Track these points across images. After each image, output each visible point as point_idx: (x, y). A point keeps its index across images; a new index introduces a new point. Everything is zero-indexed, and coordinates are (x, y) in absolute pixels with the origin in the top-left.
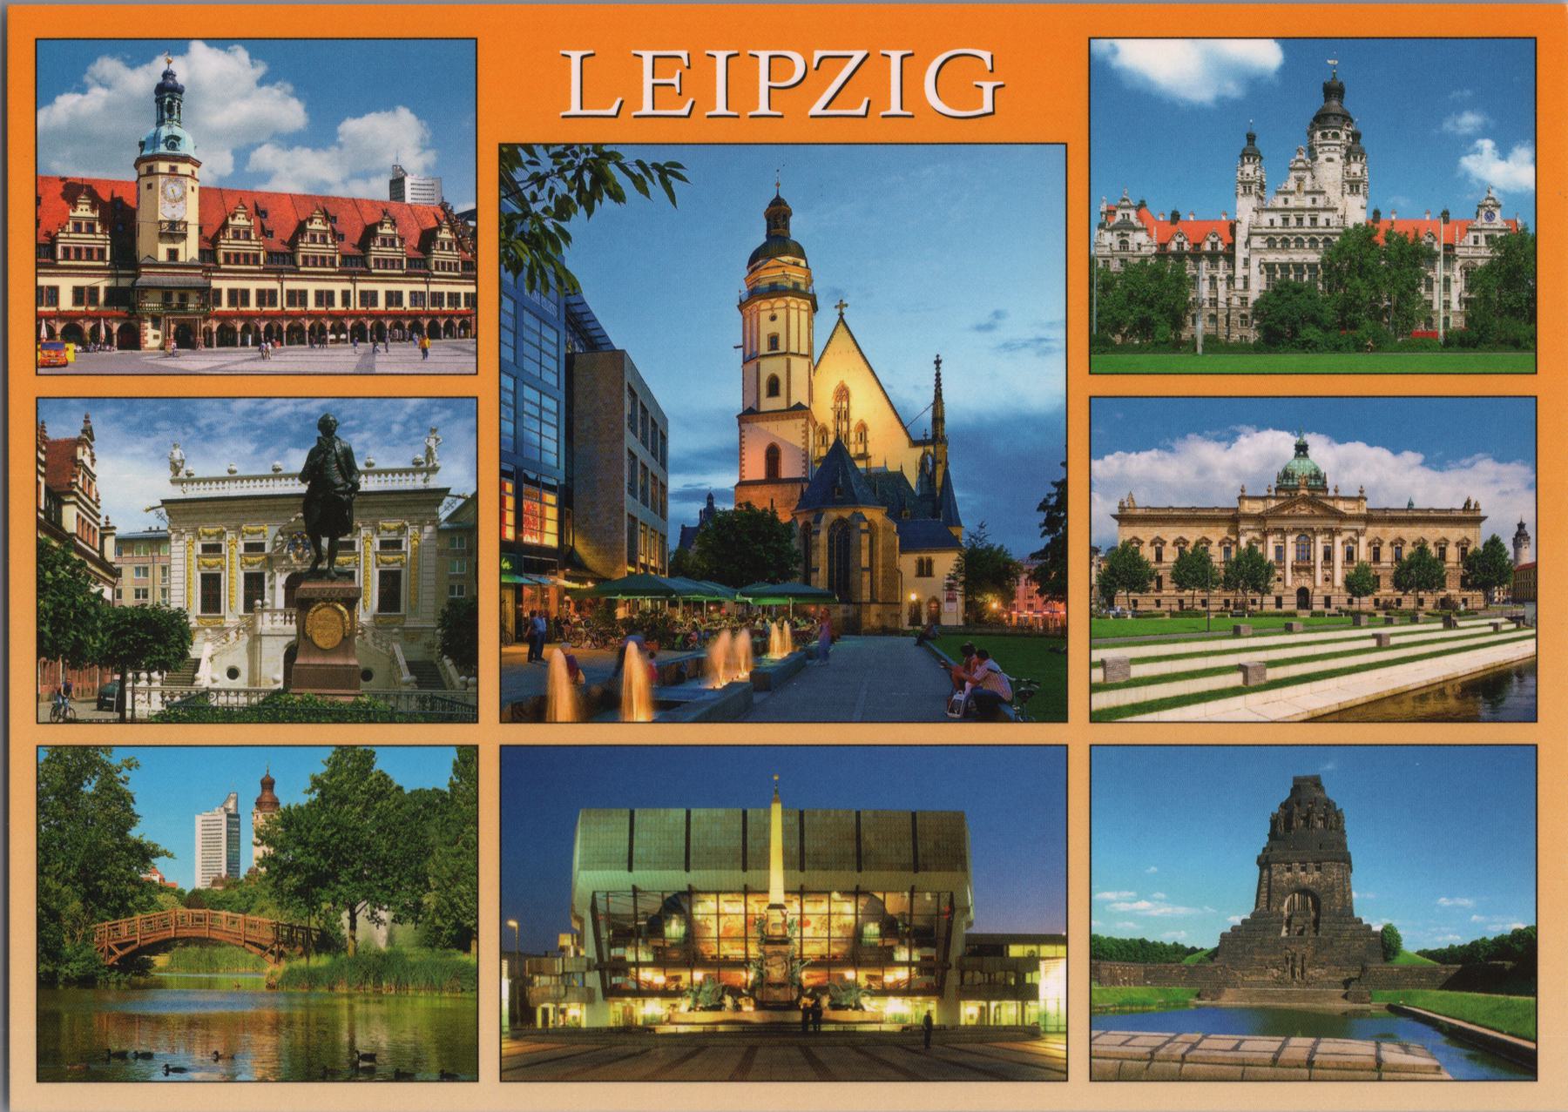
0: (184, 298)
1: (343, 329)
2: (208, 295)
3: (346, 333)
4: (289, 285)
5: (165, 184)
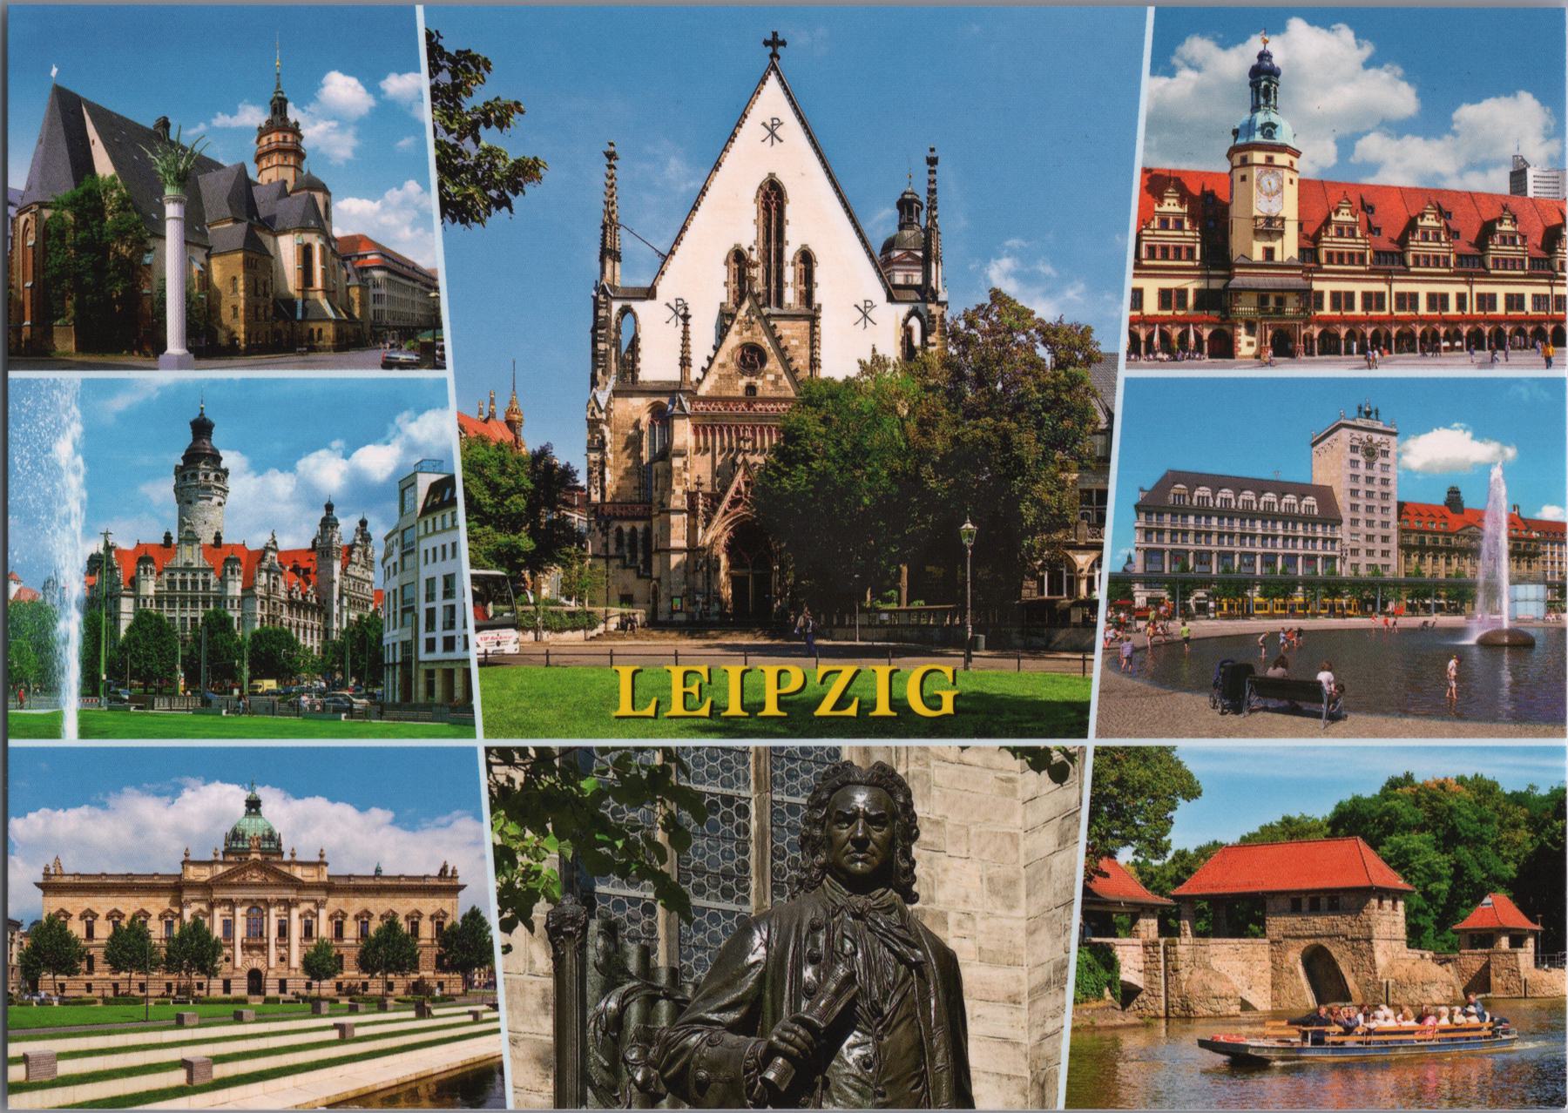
0: (1281, 302)
3: (1460, 339)
4: (1398, 287)
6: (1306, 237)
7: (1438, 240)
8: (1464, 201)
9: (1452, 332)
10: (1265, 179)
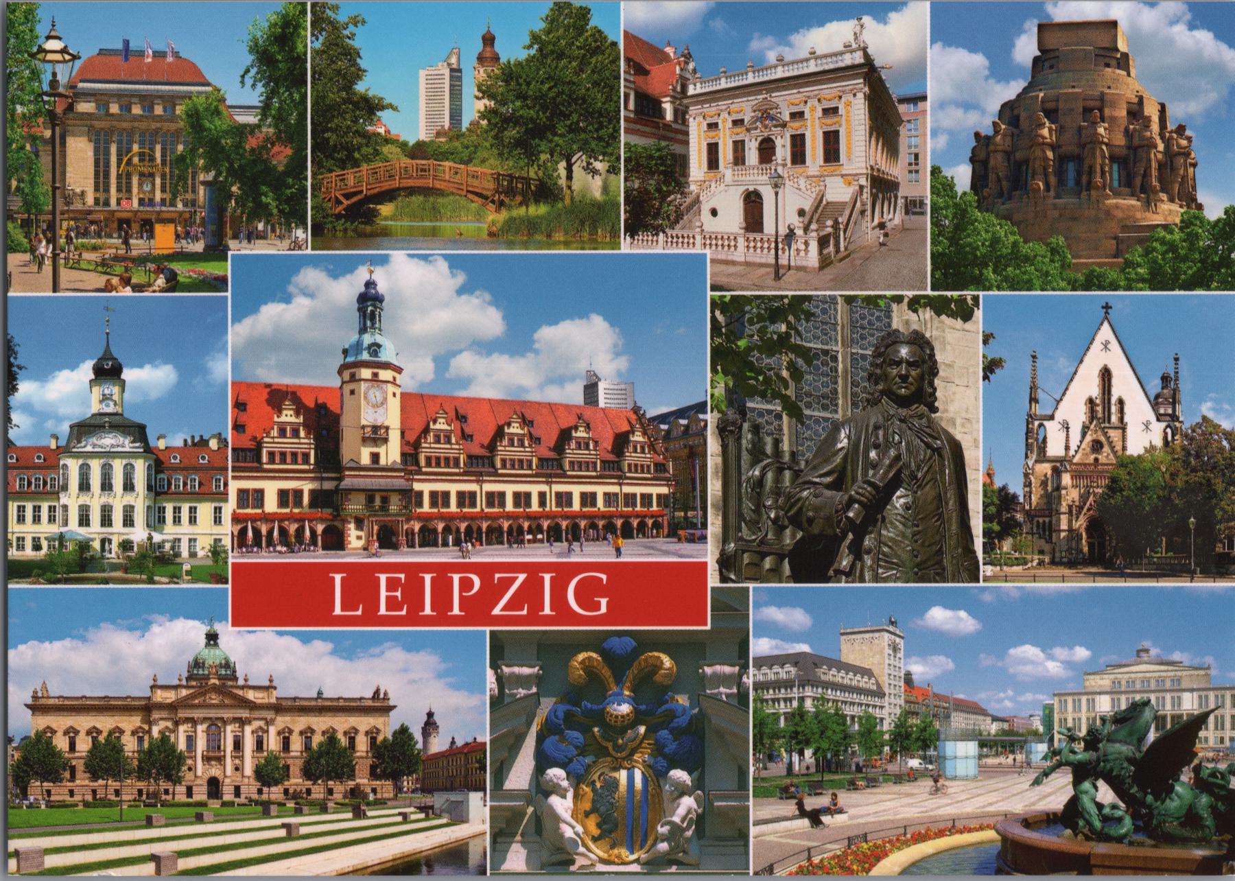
0: (385, 500)
1: (540, 529)
2: (410, 498)
3: (542, 532)
4: (488, 487)
5: (368, 389)
6: (408, 443)
7: (523, 445)
8: (544, 411)
9: (534, 527)
10: (371, 393)
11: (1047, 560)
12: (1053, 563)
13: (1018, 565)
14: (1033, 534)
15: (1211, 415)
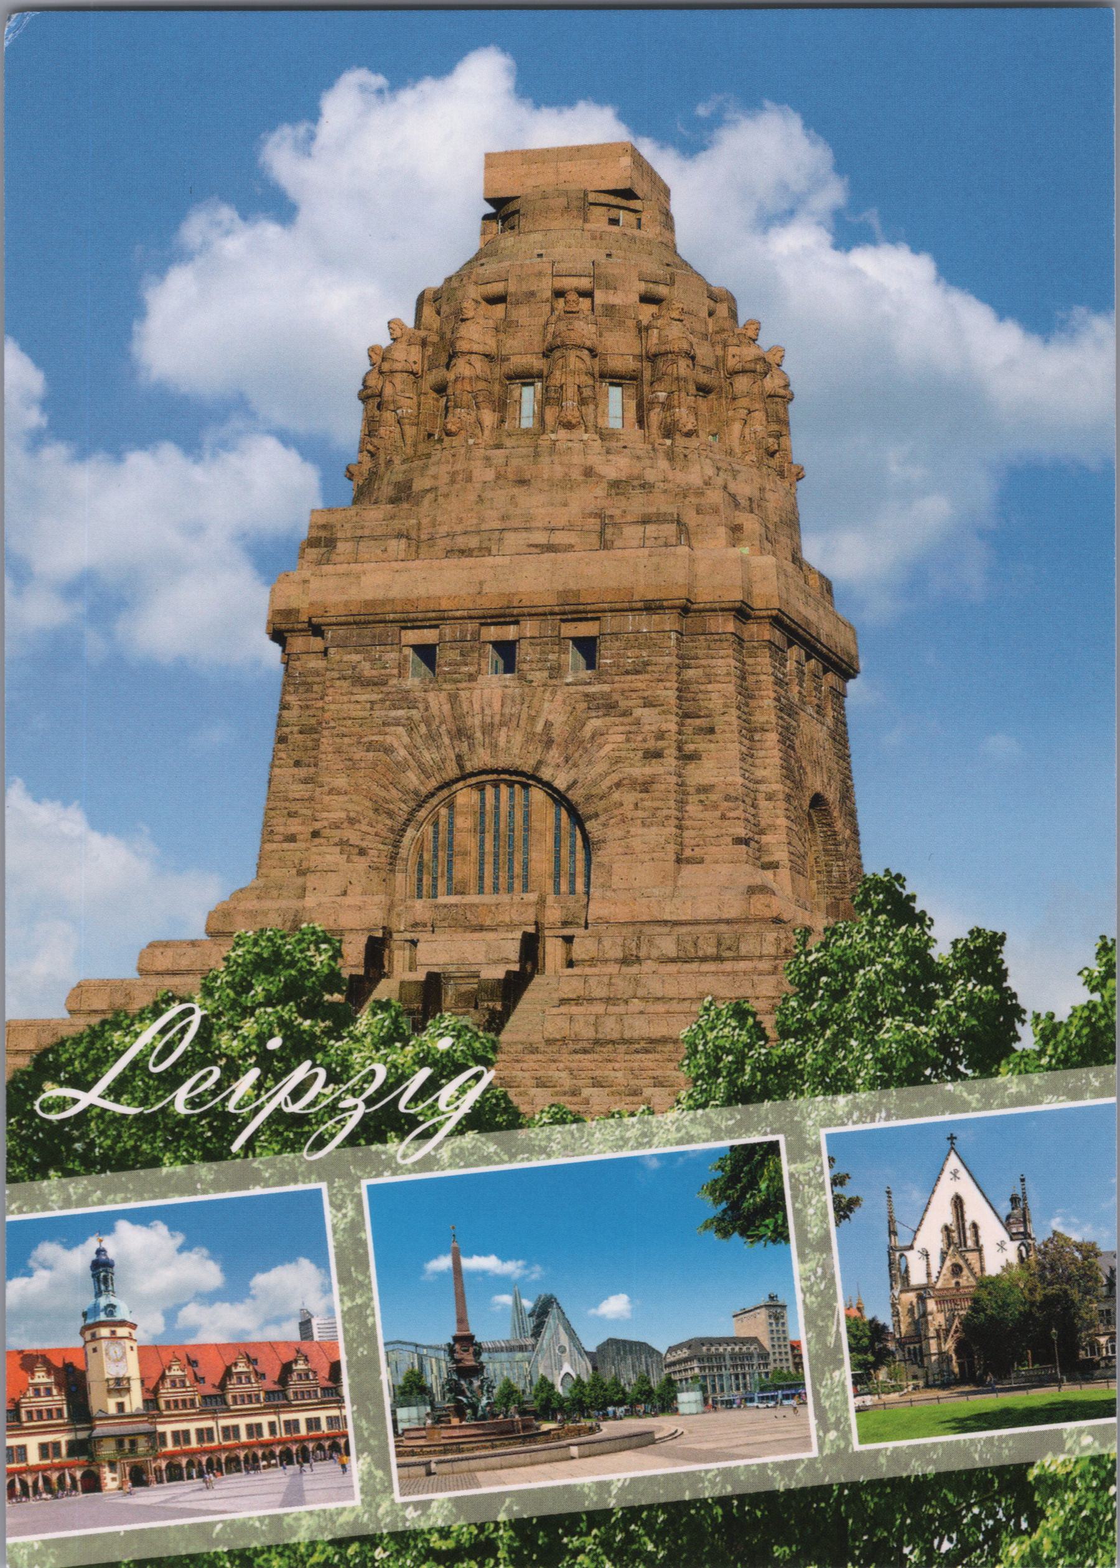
0: (133, 1443)
1: (272, 1455)
2: (155, 1438)
3: (274, 1457)
4: (223, 1422)
7: (250, 1382)
8: (267, 1349)
11: (921, 1383)
12: (928, 1386)
13: (895, 1391)
14: (905, 1361)
15: (1060, 1229)
